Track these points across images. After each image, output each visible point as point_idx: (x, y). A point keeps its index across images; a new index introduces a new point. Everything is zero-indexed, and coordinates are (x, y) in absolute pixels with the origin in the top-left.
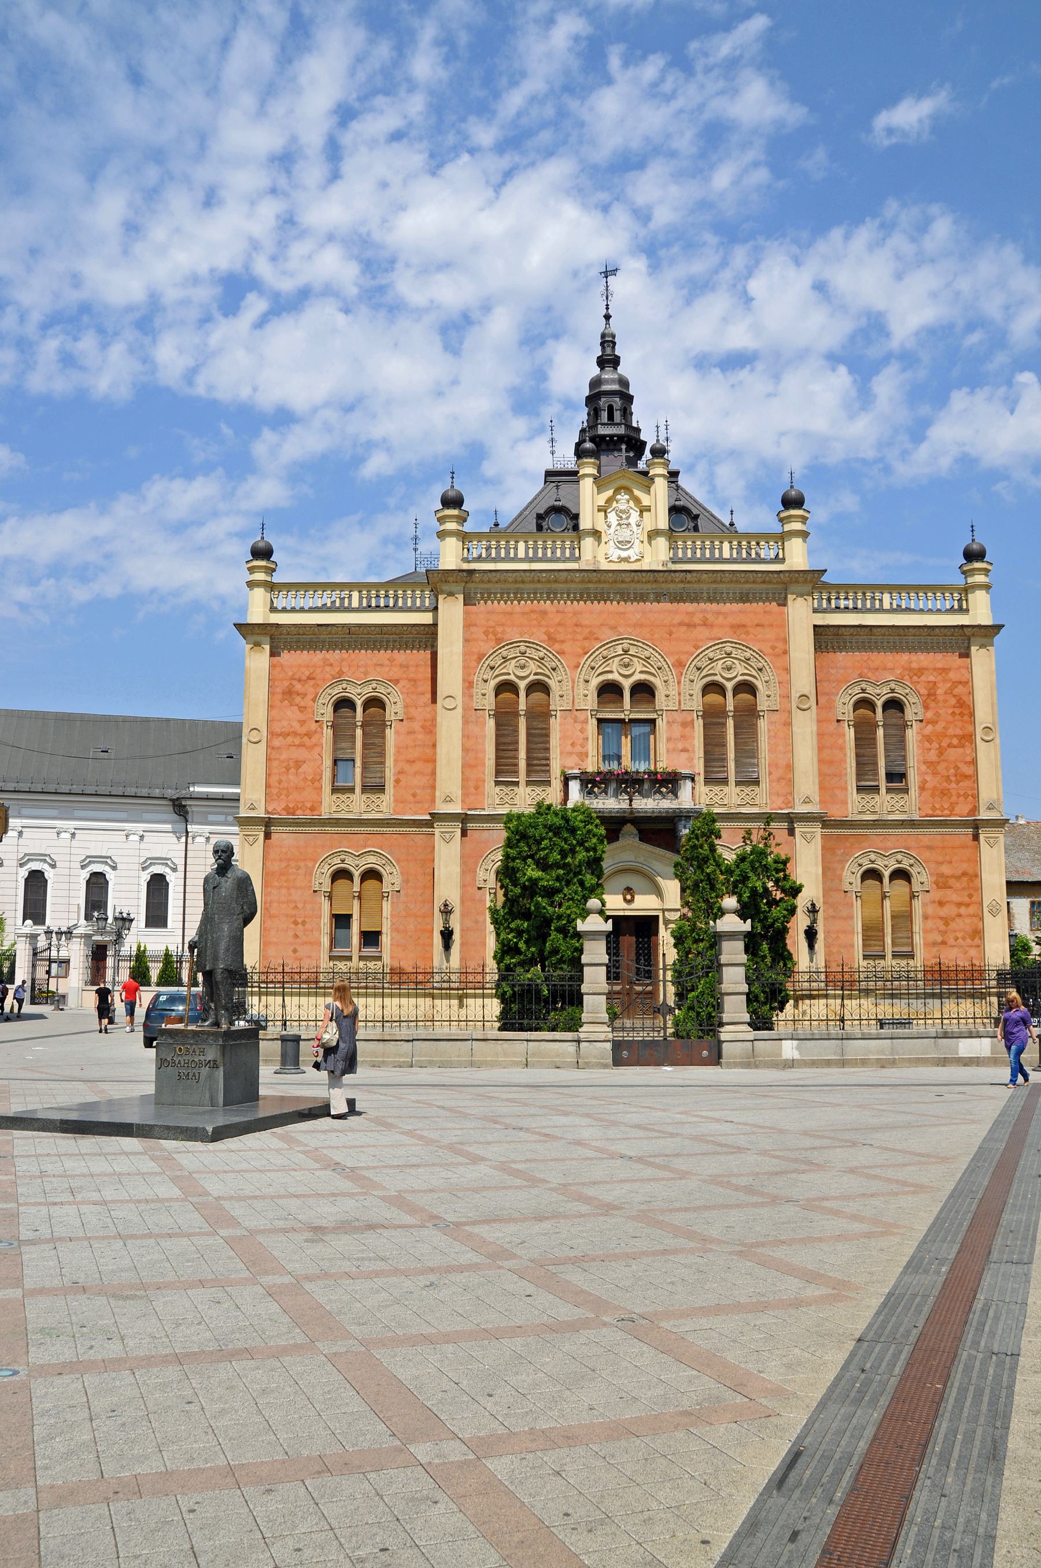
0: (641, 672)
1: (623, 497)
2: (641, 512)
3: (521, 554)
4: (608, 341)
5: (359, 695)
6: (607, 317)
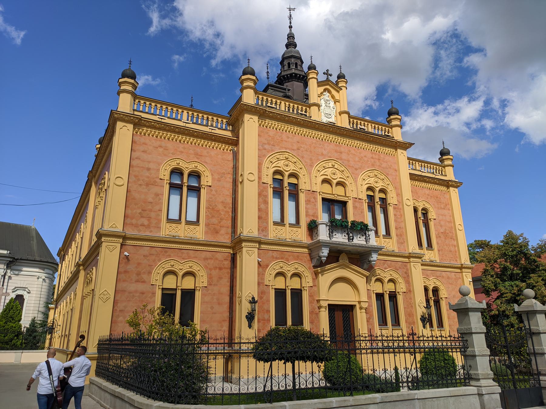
0: (340, 178)
1: (327, 94)
2: (335, 103)
3: (283, 108)
4: (291, 36)
5: (187, 167)
6: (291, 27)
